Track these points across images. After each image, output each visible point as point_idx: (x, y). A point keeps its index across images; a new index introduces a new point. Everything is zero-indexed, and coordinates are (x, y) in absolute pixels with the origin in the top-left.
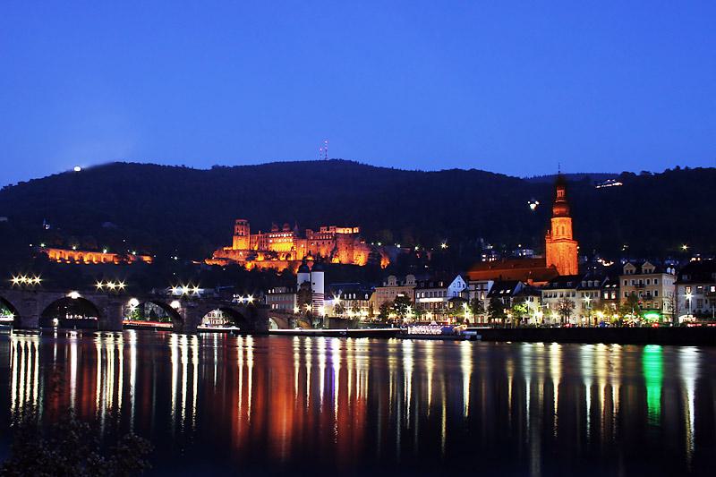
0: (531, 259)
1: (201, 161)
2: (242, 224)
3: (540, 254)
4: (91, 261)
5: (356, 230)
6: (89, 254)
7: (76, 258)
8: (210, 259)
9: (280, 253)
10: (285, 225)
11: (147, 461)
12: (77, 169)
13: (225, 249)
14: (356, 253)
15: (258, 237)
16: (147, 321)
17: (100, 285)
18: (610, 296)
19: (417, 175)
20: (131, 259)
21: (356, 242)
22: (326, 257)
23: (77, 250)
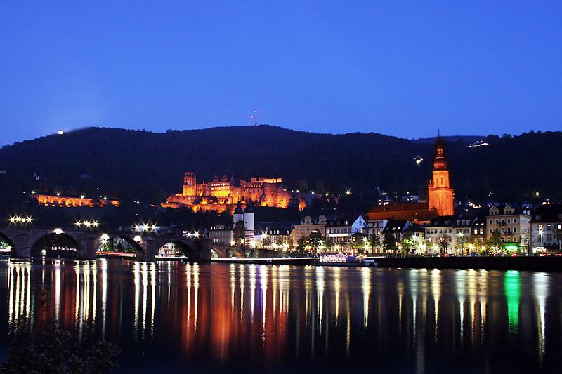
0: (417, 203)
1: (158, 126)
2: (190, 175)
3: (424, 199)
4: (71, 205)
5: (279, 181)
6: (70, 199)
7: (60, 202)
8: (165, 203)
9: (220, 198)
10: (224, 176)
11: (115, 362)
12: (61, 133)
13: (177, 195)
14: (279, 198)
15: (203, 186)
16: (115, 252)
17: (78, 224)
18: (479, 232)
19: (328, 137)
20: (103, 203)
21: (279, 190)
22: (256, 201)
23: (61, 196)
